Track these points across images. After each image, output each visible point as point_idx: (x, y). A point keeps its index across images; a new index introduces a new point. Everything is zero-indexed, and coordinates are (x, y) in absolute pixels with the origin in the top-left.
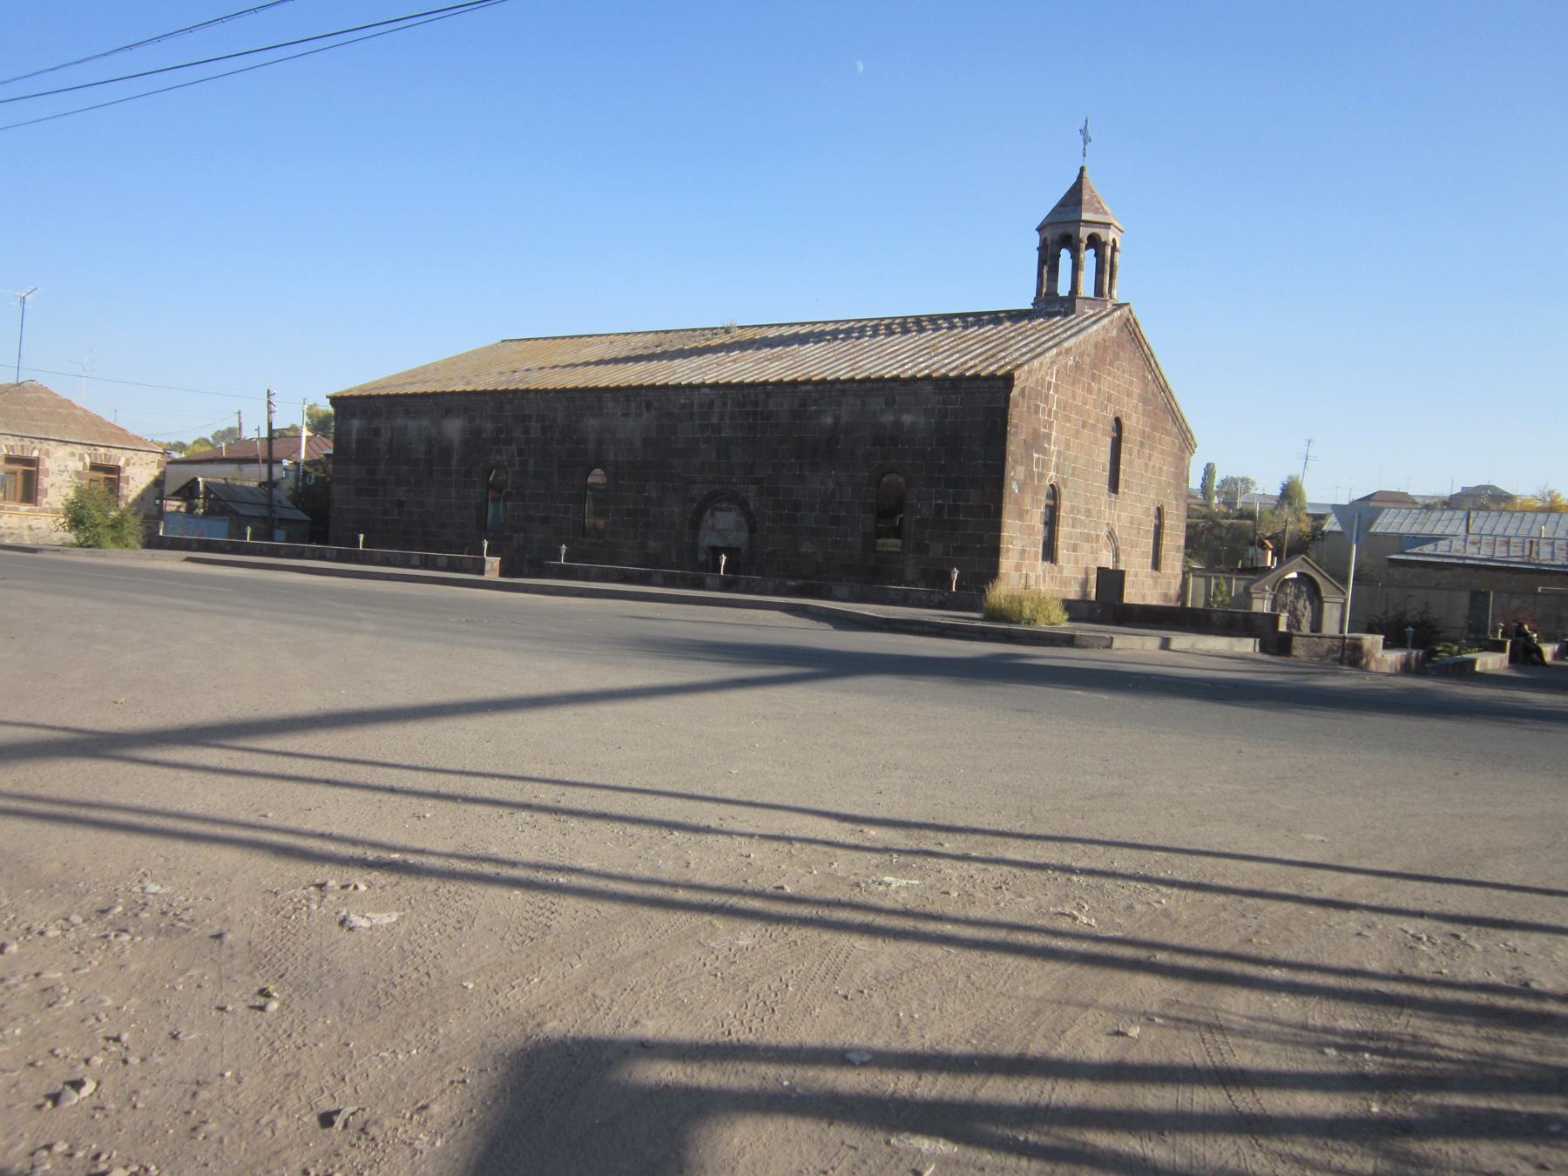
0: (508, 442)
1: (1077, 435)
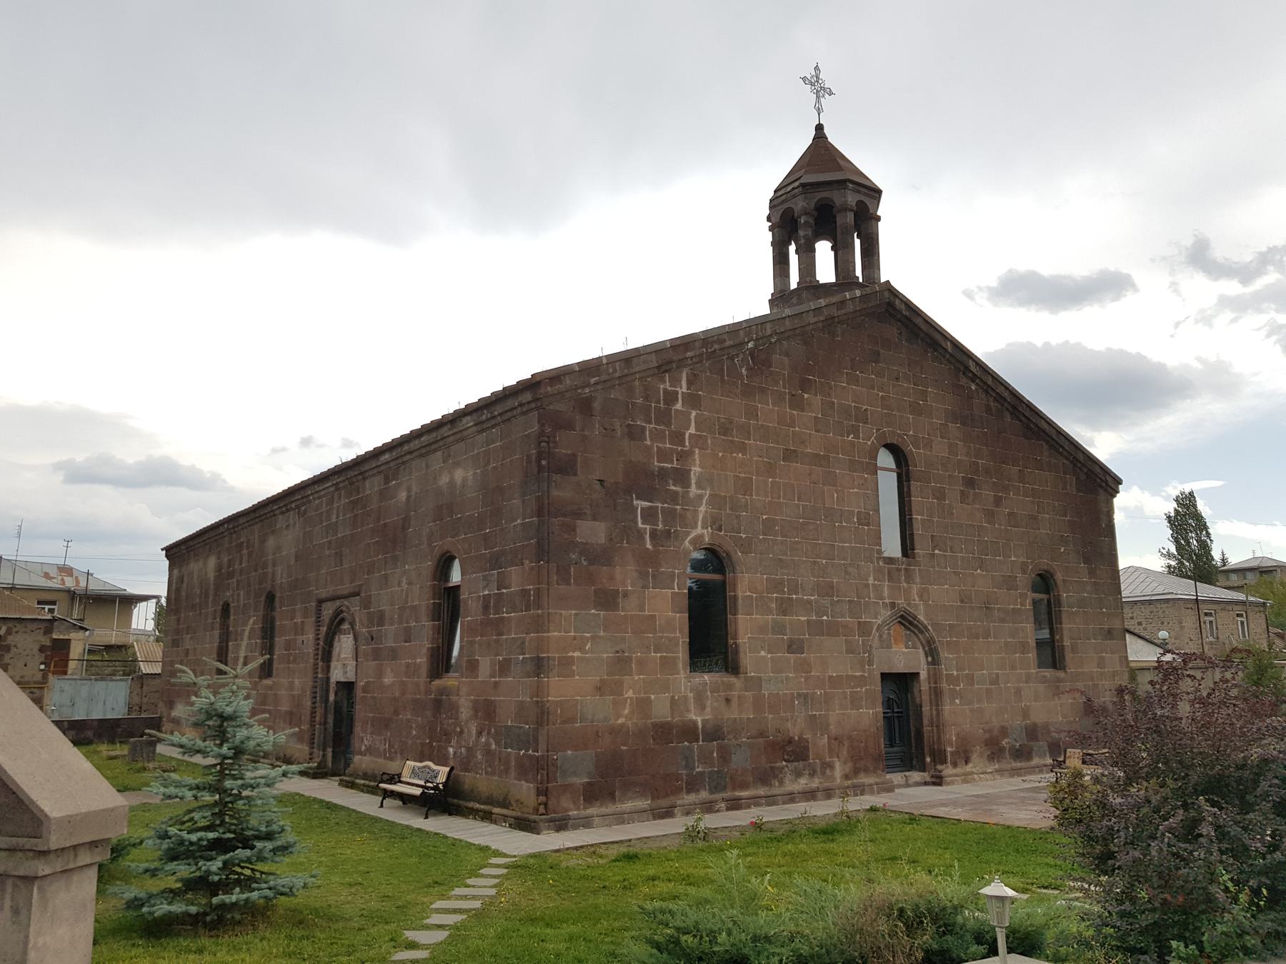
0: (231, 575)
1: (770, 470)
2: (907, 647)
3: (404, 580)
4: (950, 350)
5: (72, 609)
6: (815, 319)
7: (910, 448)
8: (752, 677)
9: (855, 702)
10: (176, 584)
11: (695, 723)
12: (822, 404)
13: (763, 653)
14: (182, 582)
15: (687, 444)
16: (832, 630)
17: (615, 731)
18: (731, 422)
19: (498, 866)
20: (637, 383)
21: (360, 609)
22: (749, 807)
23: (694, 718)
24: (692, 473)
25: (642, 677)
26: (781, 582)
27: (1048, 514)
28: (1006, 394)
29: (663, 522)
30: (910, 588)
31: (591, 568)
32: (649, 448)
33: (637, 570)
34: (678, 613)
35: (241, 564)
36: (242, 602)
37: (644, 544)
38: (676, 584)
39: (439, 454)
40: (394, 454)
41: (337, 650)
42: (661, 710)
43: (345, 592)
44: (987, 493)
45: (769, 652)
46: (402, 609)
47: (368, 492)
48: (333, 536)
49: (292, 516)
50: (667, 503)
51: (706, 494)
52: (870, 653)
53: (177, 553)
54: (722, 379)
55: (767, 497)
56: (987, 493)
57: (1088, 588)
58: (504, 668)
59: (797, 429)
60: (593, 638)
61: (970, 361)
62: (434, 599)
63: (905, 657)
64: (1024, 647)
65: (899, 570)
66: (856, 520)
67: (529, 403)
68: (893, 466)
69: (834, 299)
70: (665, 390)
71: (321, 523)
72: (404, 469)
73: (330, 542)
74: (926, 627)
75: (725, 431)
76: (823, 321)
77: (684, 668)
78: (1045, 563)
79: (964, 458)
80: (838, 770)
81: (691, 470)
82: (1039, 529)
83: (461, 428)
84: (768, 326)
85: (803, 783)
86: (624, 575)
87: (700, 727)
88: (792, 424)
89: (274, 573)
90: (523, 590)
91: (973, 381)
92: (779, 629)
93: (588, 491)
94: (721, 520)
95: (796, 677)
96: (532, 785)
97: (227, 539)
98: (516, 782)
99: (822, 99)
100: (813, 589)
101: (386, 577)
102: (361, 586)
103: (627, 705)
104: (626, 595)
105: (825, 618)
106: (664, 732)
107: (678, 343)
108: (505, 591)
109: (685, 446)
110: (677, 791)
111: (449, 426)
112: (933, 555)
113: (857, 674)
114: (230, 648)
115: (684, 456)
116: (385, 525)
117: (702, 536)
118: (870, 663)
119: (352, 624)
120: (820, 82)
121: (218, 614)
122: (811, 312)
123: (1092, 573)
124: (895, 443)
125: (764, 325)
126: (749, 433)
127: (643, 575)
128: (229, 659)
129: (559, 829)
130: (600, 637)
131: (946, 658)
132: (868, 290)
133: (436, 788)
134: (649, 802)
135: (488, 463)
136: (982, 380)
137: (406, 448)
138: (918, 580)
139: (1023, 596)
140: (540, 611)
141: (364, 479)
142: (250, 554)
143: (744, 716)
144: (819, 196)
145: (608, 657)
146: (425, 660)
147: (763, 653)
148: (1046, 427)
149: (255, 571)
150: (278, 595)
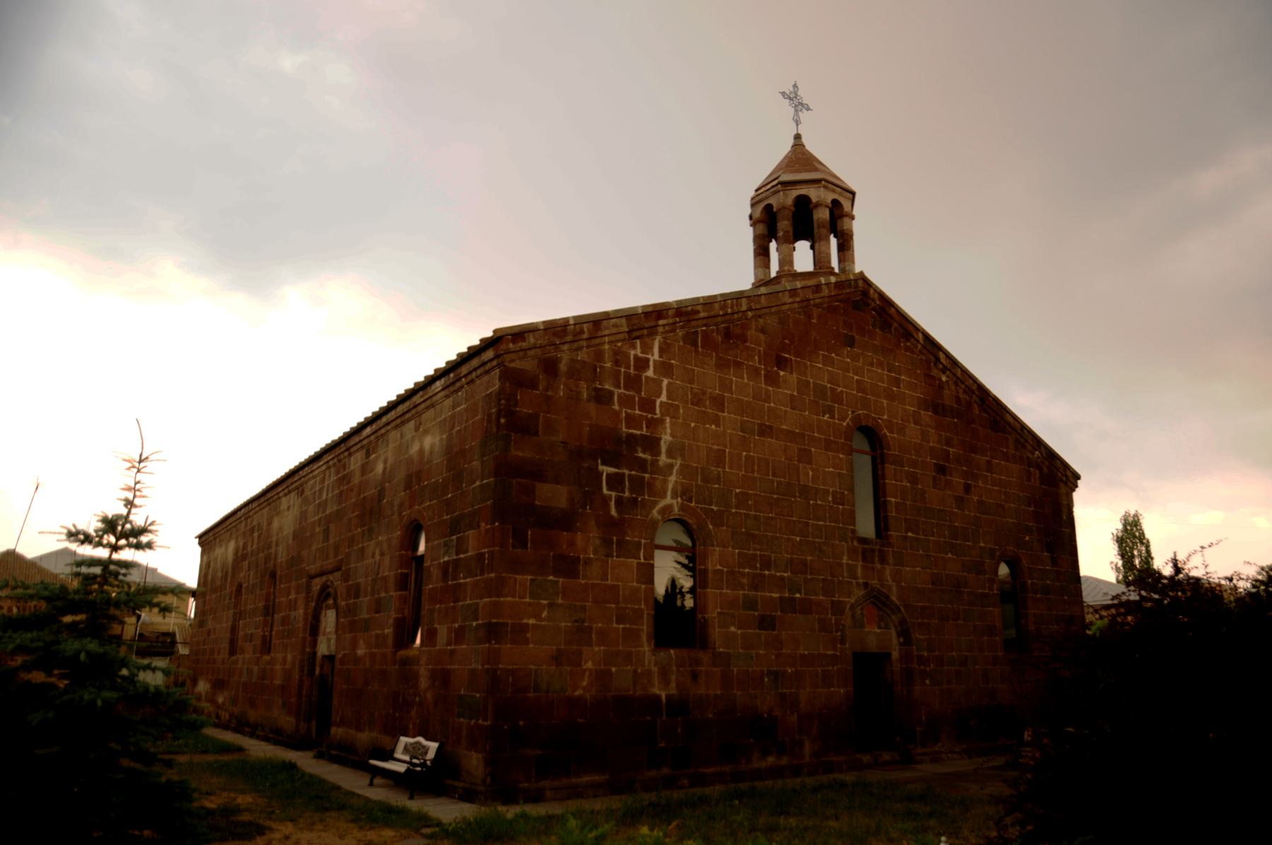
0: (244, 557)
2: (879, 627)
3: (377, 552)
4: (921, 341)
6: (791, 300)
8: (721, 653)
11: (658, 698)
12: (798, 383)
13: (733, 629)
14: (209, 567)
15: (658, 411)
16: (806, 608)
18: (704, 393)
20: (607, 347)
21: (341, 583)
23: (657, 692)
25: (602, 648)
27: (1014, 504)
28: (975, 387)
29: (629, 489)
32: (618, 413)
34: (643, 584)
35: (252, 546)
36: (251, 582)
38: (642, 554)
39: (412, 422)
40: (374, 427)
41: (324, 624)
43: (330, 567)
44: (957, 480)
45: (739, 628)
46: (374, 581)
47: (352, 467)
48: (323, 513)
49: (292, 498)
51: (676, 463)
54: (696, 351)
55: (741, 470)
58: (459, 635)
59: (772, 405)
60: (550, 605)
61: (941, 353)
62: (401, 568)
65: (873, 551)
66: (830, 499)
67: (491, 360)
68: (866, 447)
69: (810, 283)
71: (315, 501)
72: (383, 440)
73: (320, 519)
74: (898, 608)
75: (697, 401)
76: (798, 302)
77: (648, 641)
79: (935, 445)
81: (660, 439)
83: (431, 394)
84: (744, 301)
86: (587, 541)
88: (767, 400)
89: (276, 551)
90: (478, 554)
91: (944, 373)
92: (751, 604)
94: (692, 491)
96: (480, 756)
97: (244, 523)
101: (363, 549)
102: (342, 559)
104: (588, 562)
105: (798, 595)
107: (650, 309)
109: (656, 414)
111: (421, 393)
112: (906, 538)
113: (829, 653)
115: (654, 424)
116: (364, 498)
118: (843, 642)
121: (234, 593)
122: (787, 293)
124: (870, 425)
125: (739, 300)
126: (723, 405)
127: (607, 542)
128: (239, 636)
132: (843, 278)
133: (423, 765)
135: (453, 428)
136: (952, 372)
137: (384, 420)
138: (891, 560)
140: (493, 575)
141: (350, 455)
142: (259, 537)
144: (795, 193)
145: (565, 626)
146: (391, 630)
147: (733, 629)
148: (1011, 420)
149: (263, 552)
150: (279, 573)
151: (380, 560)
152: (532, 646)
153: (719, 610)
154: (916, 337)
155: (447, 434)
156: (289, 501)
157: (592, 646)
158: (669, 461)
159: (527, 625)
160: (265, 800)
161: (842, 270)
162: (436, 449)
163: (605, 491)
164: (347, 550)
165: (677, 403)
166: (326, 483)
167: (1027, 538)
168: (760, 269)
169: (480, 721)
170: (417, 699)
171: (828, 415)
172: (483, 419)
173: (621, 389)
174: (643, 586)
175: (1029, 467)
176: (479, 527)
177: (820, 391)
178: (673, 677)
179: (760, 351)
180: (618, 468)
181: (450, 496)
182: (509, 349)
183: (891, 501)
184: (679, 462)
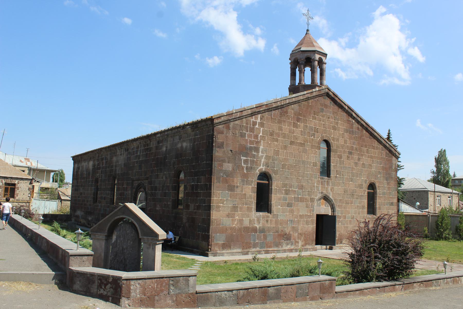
0: (99, 168)
1: (285, 147)
2: (325, 206)
5: (30, 173)
7: (331, 141)
9: (307, 223)
10: (76, 170)
11: (256, 227)
12: (304, 126)
13: (279, 207)
14: (79, 169)
15: (259, 139)
16: (302, 200)
17: (232, 229)
19: (199, 264)
21: (148, 185)
22: (272, 253)
23: (256, 226)
24: (260, 148)
25: (241, 213)
26: (287, 184)
28: (364, 124)
29: (250, 164)
30: (328, 187)
31: (227, 178)
32: (247, 140)
33: (241, 179)
36: (103, 178)
37: (244, 171)
42: (246, 223)
44: (356, 157)
45: (281, 206)
47: (151, 146)
48: (138, 159)
49: (123, 151)
50: (251, 158)
52: (313, 208)
53: (77, 159)
54: (272, 118)
55: (284, 156)
56: (356, 157)
57: (386, 189)
59: (295, 134)
63: (325, 210)
64: (363, 207)
65: (325, 181)
68: (326, 147)
70: (253, 121)
71: (134, 154)
73: (137, 161)
75: (271, 134)
78: (373, 180)
80: (300, 243)
82: (372, 169)
85: (289, 247)
86: (237, 181)
87: (258, 229)
88: (293, 133)
90: (205, 184)
92: (285, 199)
93: (227, 154)
95: (289, 215)
96: (206, 243)
98: (201, 242)
99: (309, 21)
100: (297, 187)
103: (236, 221)
104: (237, 187)
105: (300, 196)
106: (247, 229)
108: (199, 184)
110: (250, 247)
112: (336, 177)
113: (309, 214)
114: (99, 193)
115: (258, 143)
117: (262, 169)
119: (145, 189)
120: (309, 15)
123: (388, 184)
124: (327, 139)
127: (243, 181)
129: (214, 256)
130: (228, 200)
131: (338, 210)
134: (241, 250)
135: (195, 142)
138: (331, 185)
139: (365, 190)
142: (106, 162)
143: (272, 226)
147: (279, 207)
151: (165, 180)
152: (221, 212)
153: (275, 201)
154: (345, 107)
155: (192, 144)
156: (121, 152)
157: (238, 212)
158: (262, 154)
159: (220, 205)
160: (103, 255)
161: (321, 83)
162: (188, 148)
163: (243, 165)
164: (150, 174)
165: (265, 136)
166: (139, 149)
167: (379, 176)
168: (292, 81)
169: (206, 233)
170: (182, 225)
171: (313, 137)
172: (206, 142)
173: (248, 132)
174: (253, 194)
175: (382, 151)
176: (205, 176)
177: (311, 128)
178: (261, 222)
179: (292, 116)
180: (247, 158)
181: (194, 164)
182: (216, 122)
183: (332, 165)
184: (265, 155)
